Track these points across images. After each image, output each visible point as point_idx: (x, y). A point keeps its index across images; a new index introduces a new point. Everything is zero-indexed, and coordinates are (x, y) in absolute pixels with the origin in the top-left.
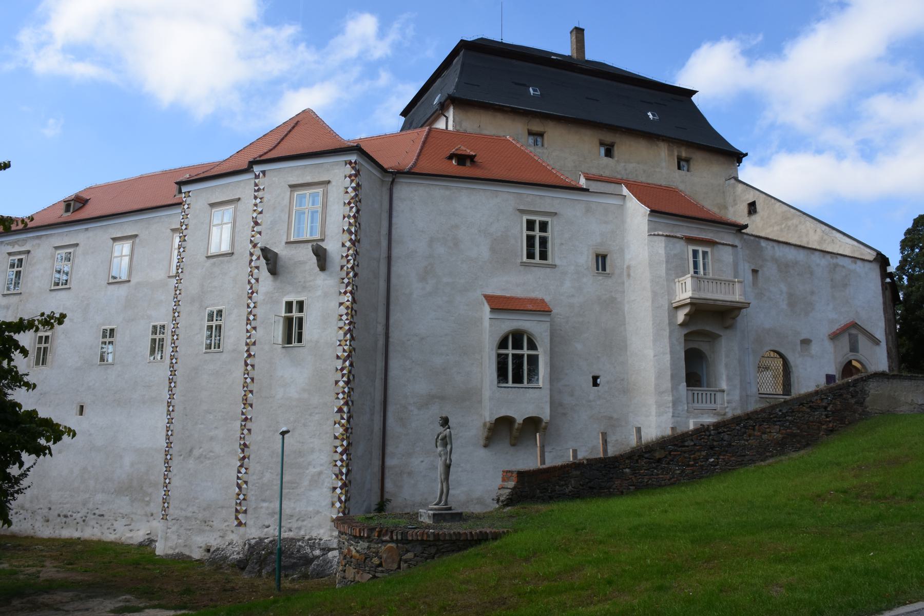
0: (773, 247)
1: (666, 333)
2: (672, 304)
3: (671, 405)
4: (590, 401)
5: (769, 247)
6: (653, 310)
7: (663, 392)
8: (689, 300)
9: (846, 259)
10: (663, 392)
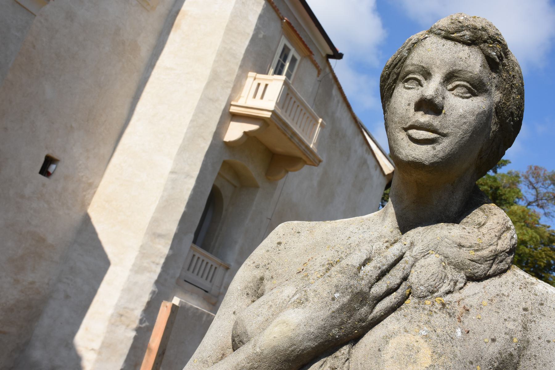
0: (338, 102)
1: (205, 145)
2: (231, 105)
3: (162, 261)
4: (22, 197)
5: (336, 99)
6: (201, 100)
7: (160, 236)
8: (270, 114)
9: (373, 159)
10: (160, 236)
